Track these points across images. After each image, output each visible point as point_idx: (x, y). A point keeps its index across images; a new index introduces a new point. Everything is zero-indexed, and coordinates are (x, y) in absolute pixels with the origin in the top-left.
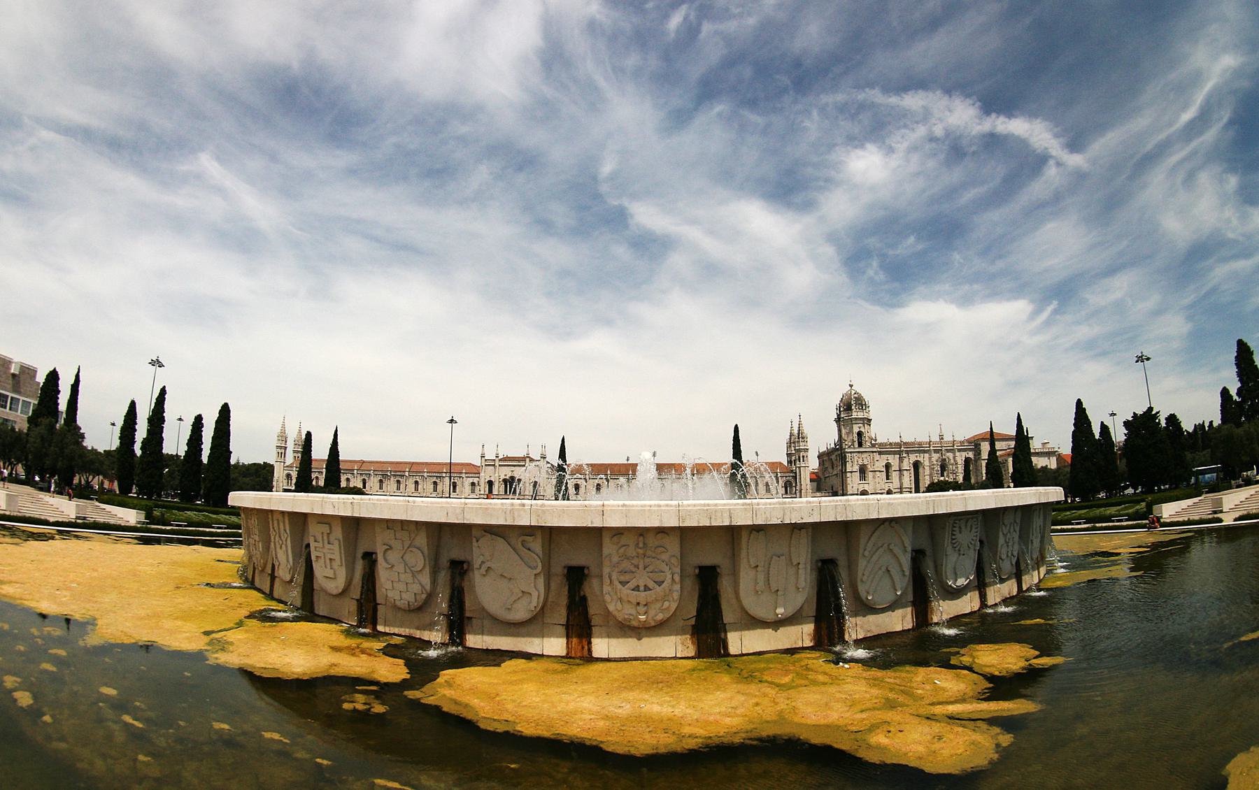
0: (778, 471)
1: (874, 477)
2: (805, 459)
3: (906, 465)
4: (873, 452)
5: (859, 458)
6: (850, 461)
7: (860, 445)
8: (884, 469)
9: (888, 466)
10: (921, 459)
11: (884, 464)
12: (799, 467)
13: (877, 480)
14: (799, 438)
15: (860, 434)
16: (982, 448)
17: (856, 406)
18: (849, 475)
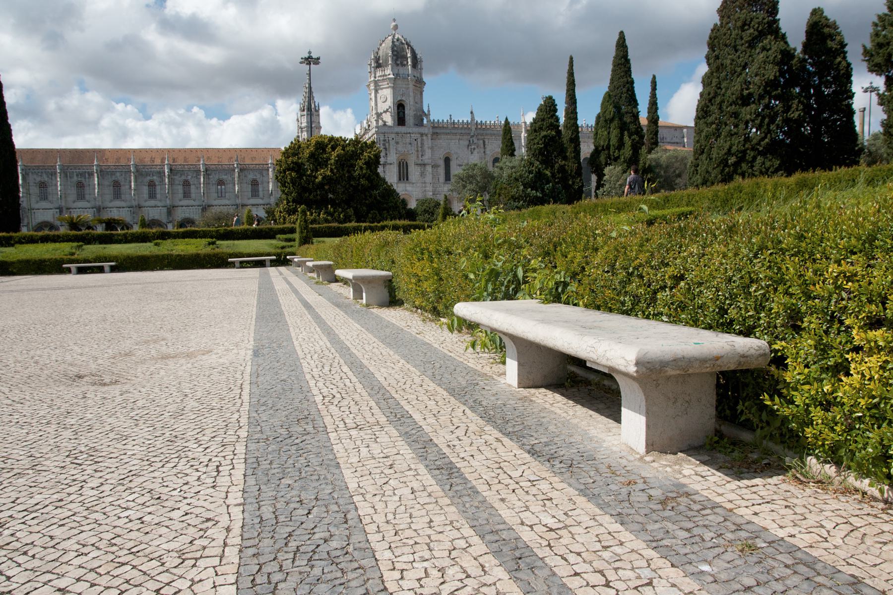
1: (422, 174)
4: (422, 135)
5: (397, 143)
8: (442, 163)
9: (447, 160)
11: (440, 155)
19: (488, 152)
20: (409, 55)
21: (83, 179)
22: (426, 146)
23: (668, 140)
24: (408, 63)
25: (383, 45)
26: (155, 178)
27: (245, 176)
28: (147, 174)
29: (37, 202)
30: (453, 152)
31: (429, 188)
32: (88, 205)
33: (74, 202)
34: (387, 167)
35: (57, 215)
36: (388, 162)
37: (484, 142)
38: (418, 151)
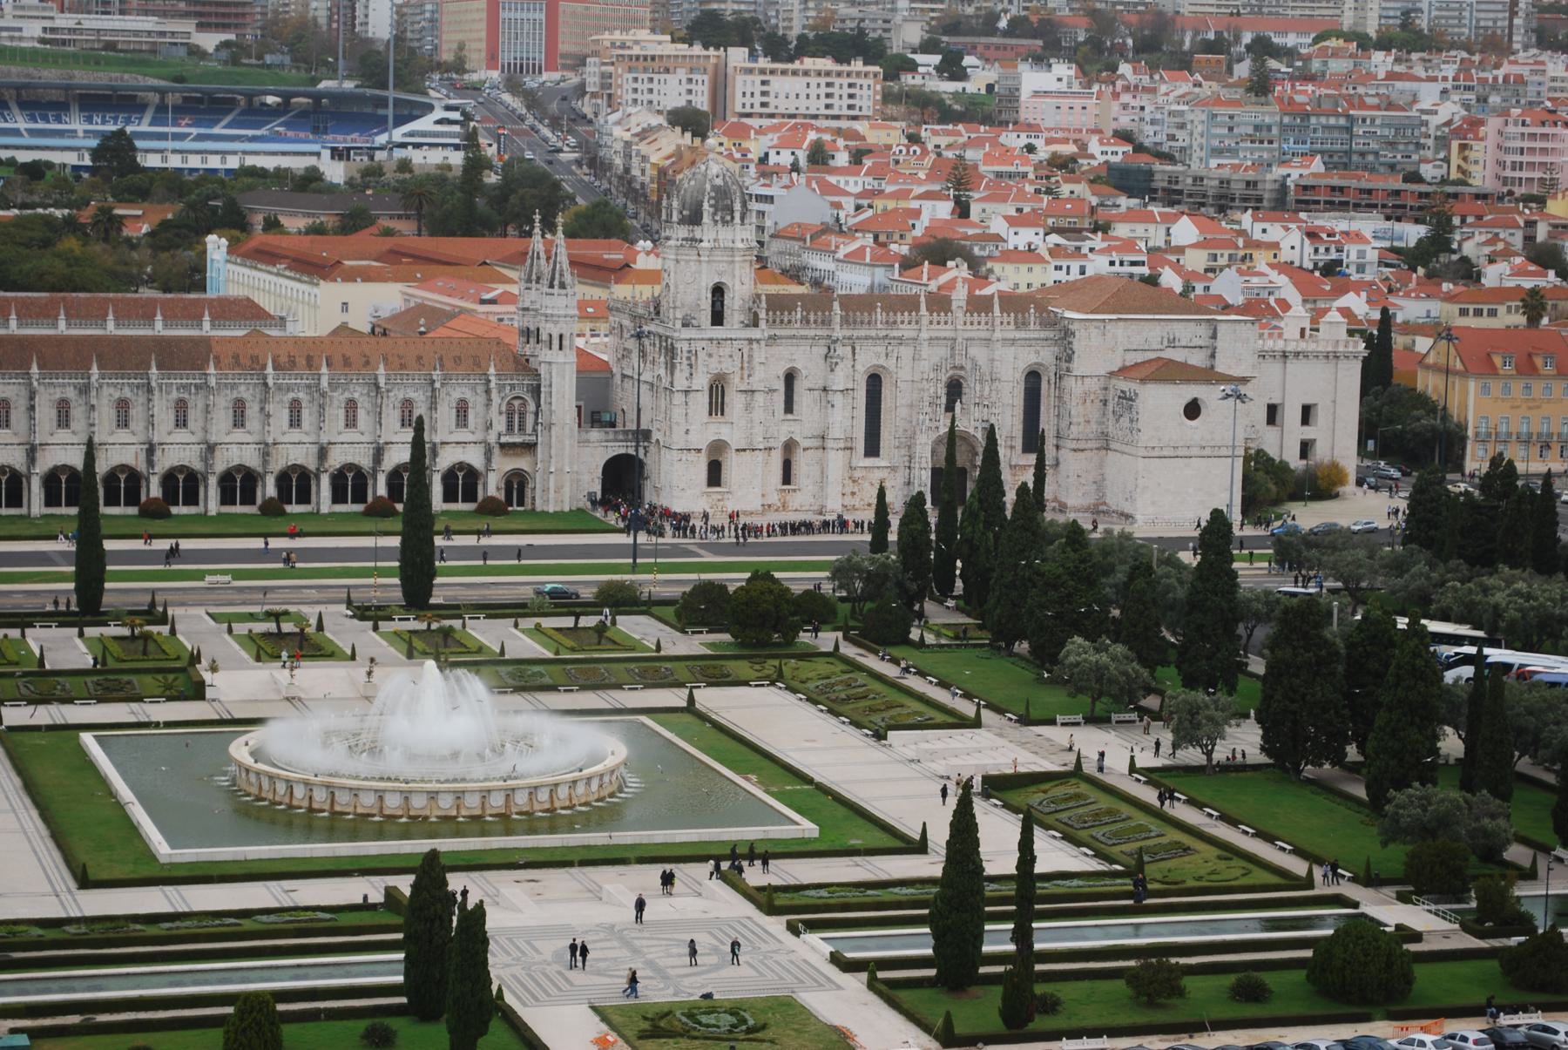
0: (492, 371)
1: (748, 408)
2: (564, 342)
3: (839, 380)
4: (750, 341)
5: (710, 355)
6: (685, 362)
7: (718, 318)
9: (790, 378)
10: (890, 364)
11: (781, 373)
12: (550, 363)
13: (758, 414)
14: (551, 286)
15: (718, 291)
16: (1077, 345)
17: (715, 214)
18: (679, 398)
19: (859, 367)
20: (737, 206)
21: (186, 396)
22: (757, 360)
23: (1184, 344)
24: (733, 218)
25: (693, 183)
26: (301, 395)
27: (448, 394)
28: (289, 389)
29: (113, 433)
30: (799, 366)
31: (758, 430)
32: (193, 439)
33: (169, 433)
34: (692, 395)
35: (143, 457)
36: (694, 388)
37: (854, 349)
38: (742, 368)
